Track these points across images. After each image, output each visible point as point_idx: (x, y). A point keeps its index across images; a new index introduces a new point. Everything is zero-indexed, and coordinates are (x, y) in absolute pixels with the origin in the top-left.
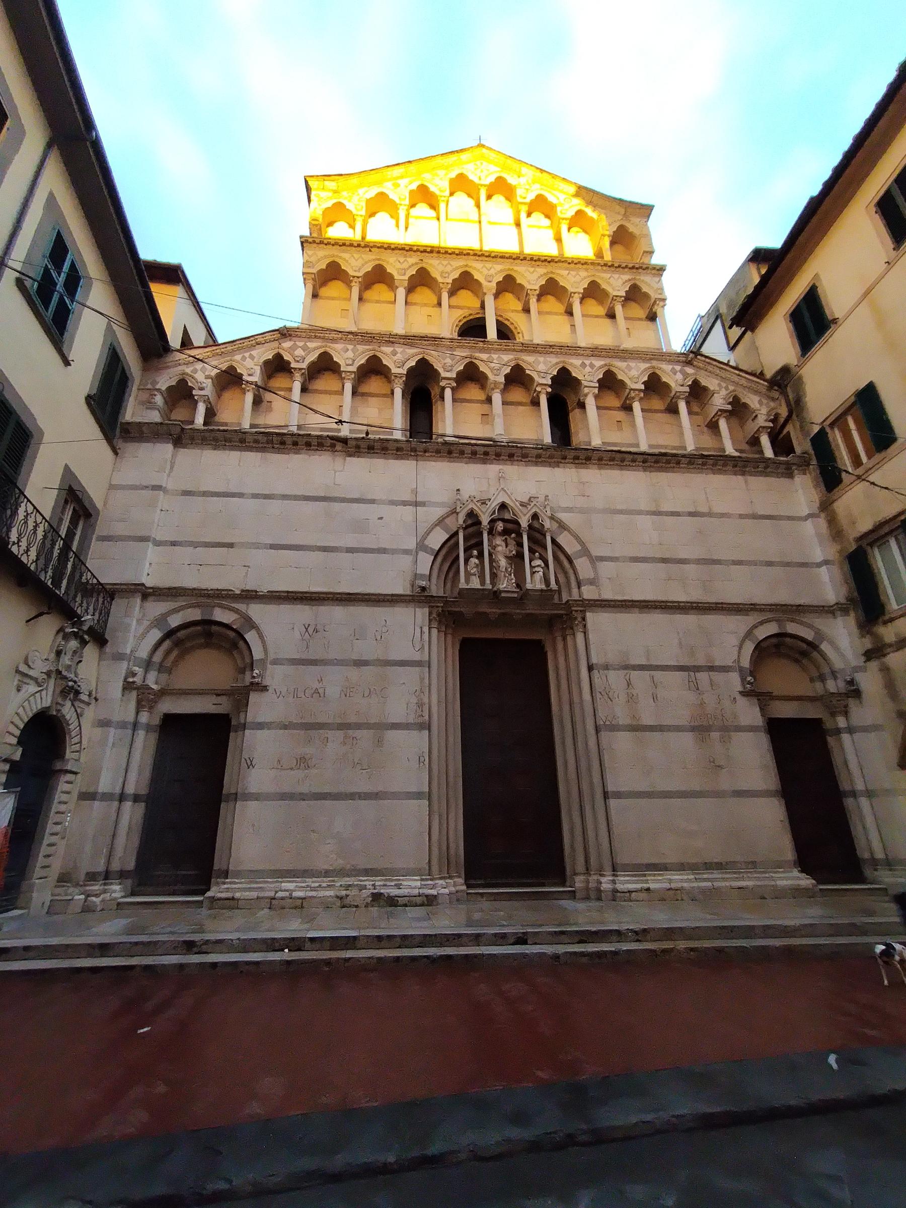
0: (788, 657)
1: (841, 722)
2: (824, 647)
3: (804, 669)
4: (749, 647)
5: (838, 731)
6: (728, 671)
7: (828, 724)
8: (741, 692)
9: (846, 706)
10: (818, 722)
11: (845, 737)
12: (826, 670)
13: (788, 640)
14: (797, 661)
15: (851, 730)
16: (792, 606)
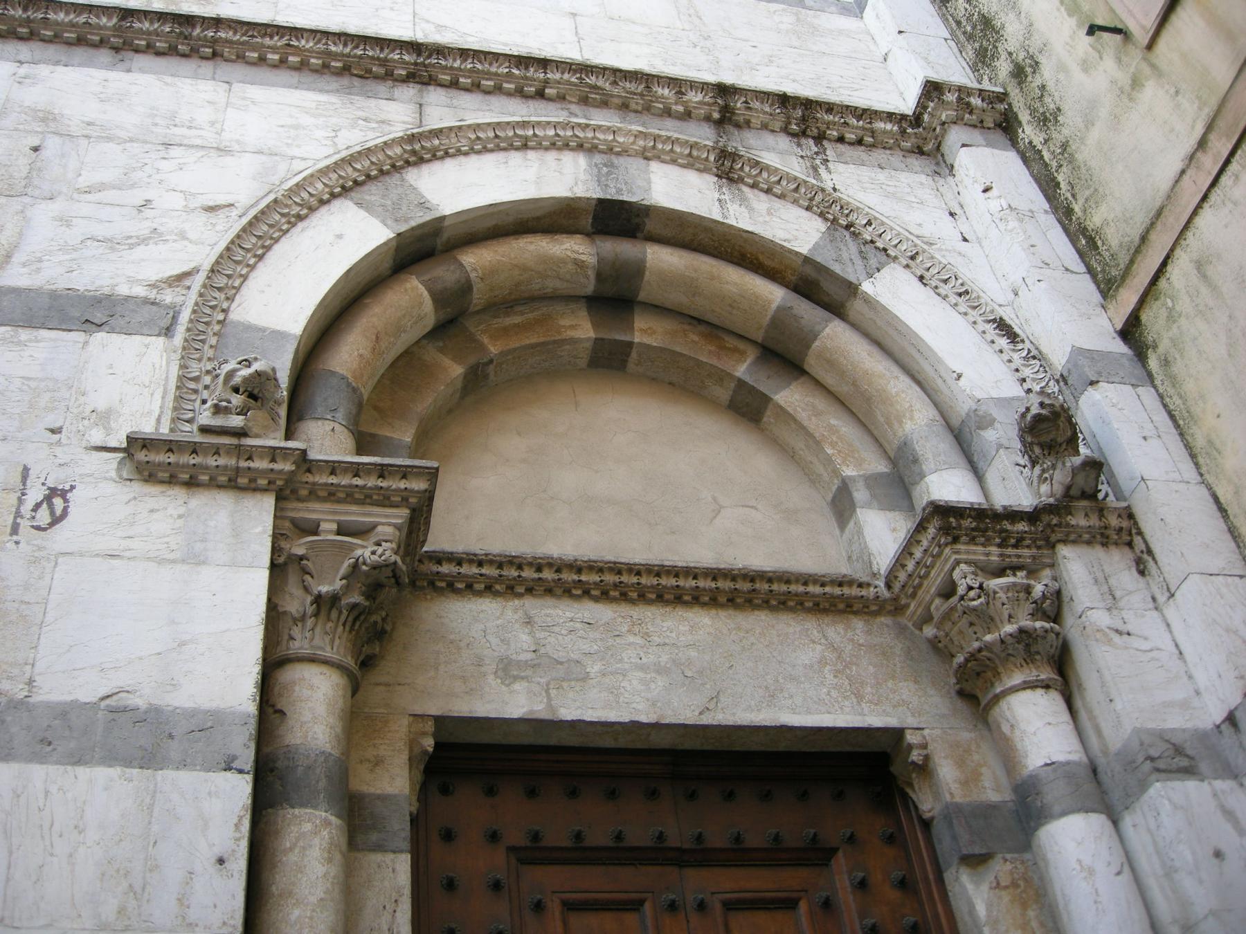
0: (678, 381)
1: (1037, 728)
2: (891, 290)
3: (794, 447)
4: (351, 236)
5: (1026, 810)
6: (90, 325)
7: (953, 778)
8: (137, 444)
9: (1053, 607)
10: (867, 769)
11: (1072, 840)
12: (916, 421)
13: (661, 259)
14: (749, 409)
15: (1102, 787)
16: (678, 84)
